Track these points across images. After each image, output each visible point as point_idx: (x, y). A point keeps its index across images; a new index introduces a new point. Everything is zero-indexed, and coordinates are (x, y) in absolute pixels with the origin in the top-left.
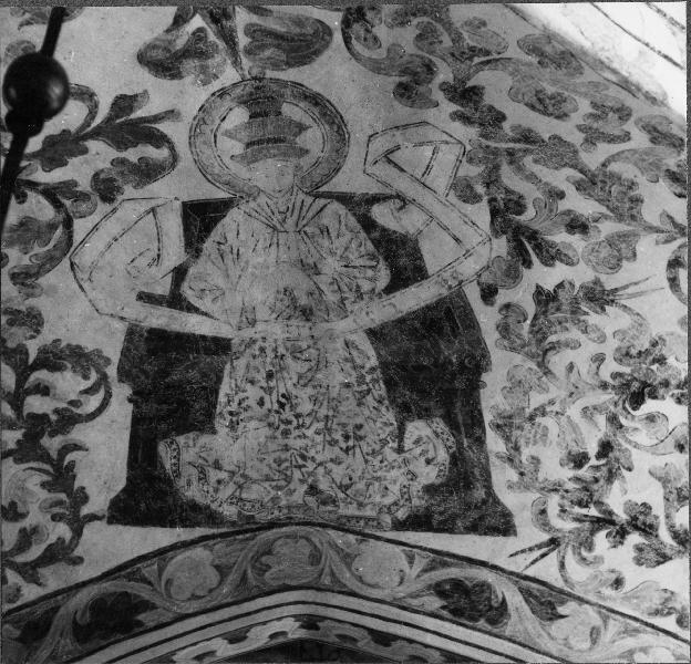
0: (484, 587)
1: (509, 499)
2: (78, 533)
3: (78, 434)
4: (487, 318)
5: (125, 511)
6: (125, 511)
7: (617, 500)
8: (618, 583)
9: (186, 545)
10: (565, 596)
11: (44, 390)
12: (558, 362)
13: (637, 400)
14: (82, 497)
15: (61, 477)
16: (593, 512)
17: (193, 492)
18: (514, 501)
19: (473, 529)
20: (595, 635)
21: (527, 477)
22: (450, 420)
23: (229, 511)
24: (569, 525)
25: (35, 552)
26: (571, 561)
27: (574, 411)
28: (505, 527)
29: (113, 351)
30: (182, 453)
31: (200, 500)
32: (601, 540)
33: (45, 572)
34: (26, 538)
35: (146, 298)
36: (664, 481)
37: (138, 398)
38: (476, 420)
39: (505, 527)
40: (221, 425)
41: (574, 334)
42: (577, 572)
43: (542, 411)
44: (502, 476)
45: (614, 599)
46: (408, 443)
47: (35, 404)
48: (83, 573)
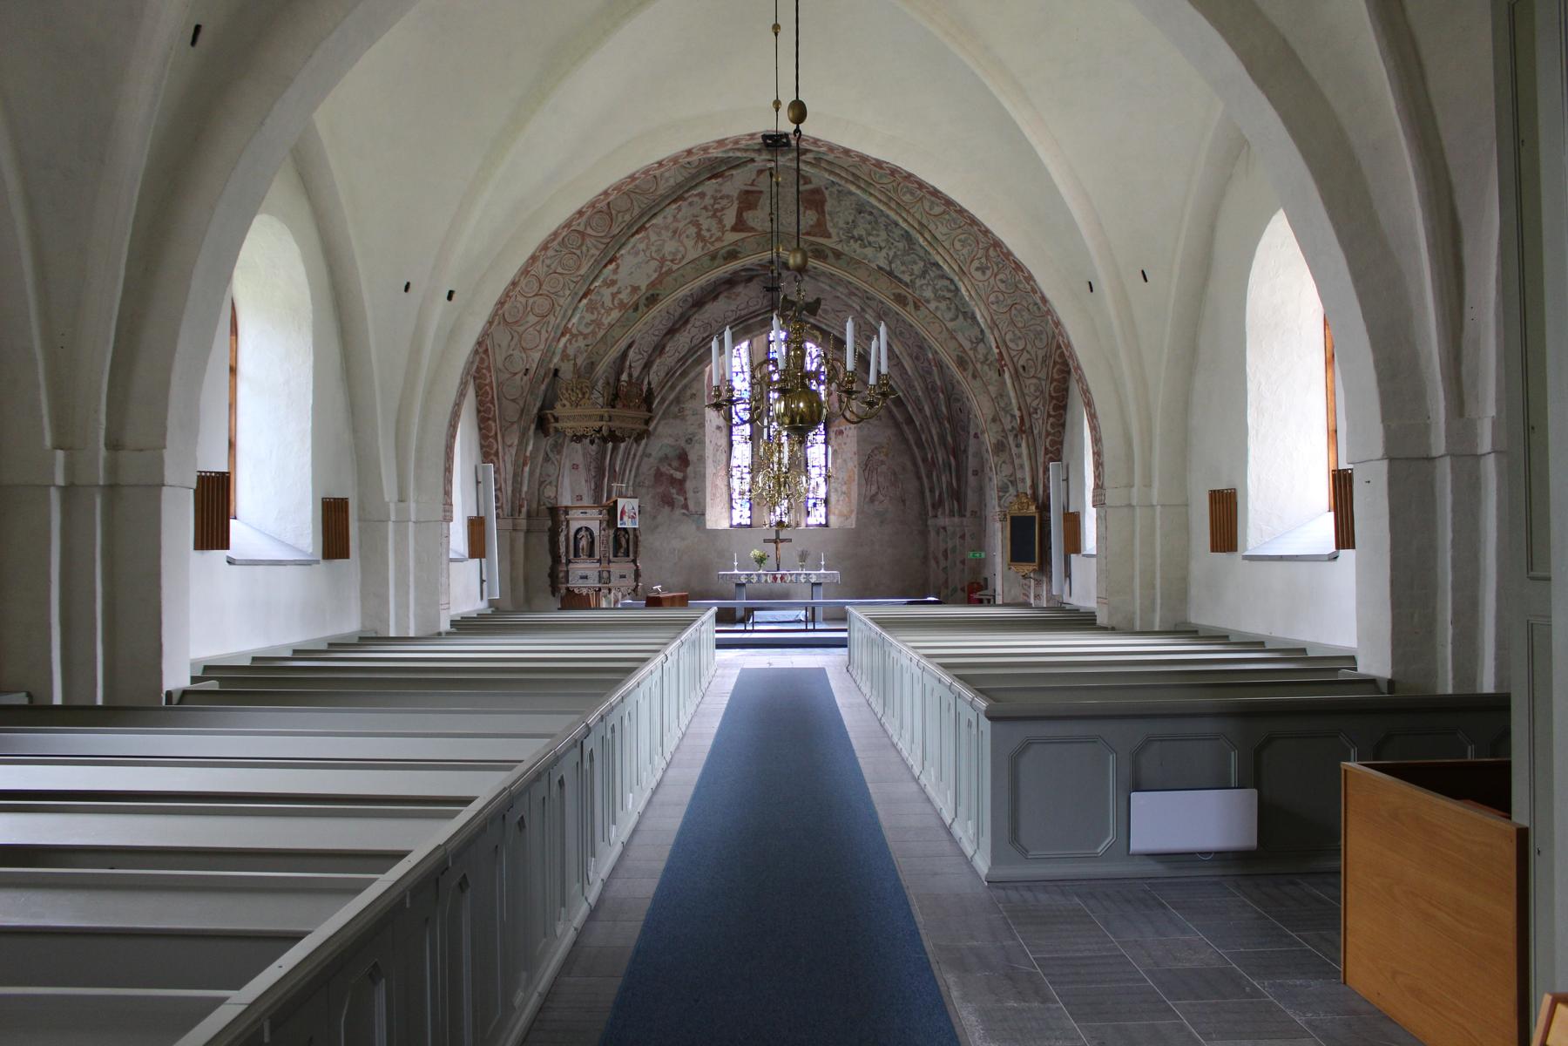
0: (823, 251)
1: (831, 230)
2: (723, 234)
3: (726, 212)
4: (827, 193)
5: (735, 229)
6: (735, 229)
7: (855, 233)
8: (855, 252)
9: (749, 237)
10: (843, 254)
11: (719, 203)
12: (843, 203)
13: (860, 213)
14: (724, 226)
15: (720, 221)
16: (850, 235)
17: (751, 223)
18: (832, 231)
19: (821, 236)
20: (848, 264)
21: (835, 226)
22: (817, 211)
23: (760, 229)
24: (844, 237)
25: (713, 240)
26: (845, 246)
27: (846, 213)
28: (829, 236)
29: (736, 195)
30: (748, 215)
31: (753, 226)
32: (852, 241)
33: (716, 243)
34: (711, 237)
35: (746, 185)
36: (866, 230)
37: (740, 203)
38: (823, 212)
39: (829, 236)
40: (758, 208)
41: (845, 198)
42: (846, 248)
43: (839, 212)
44: (829, 225)
45: (853, 255)
46: (806, 215)
47: (716, 206)
48: (725, 243)
